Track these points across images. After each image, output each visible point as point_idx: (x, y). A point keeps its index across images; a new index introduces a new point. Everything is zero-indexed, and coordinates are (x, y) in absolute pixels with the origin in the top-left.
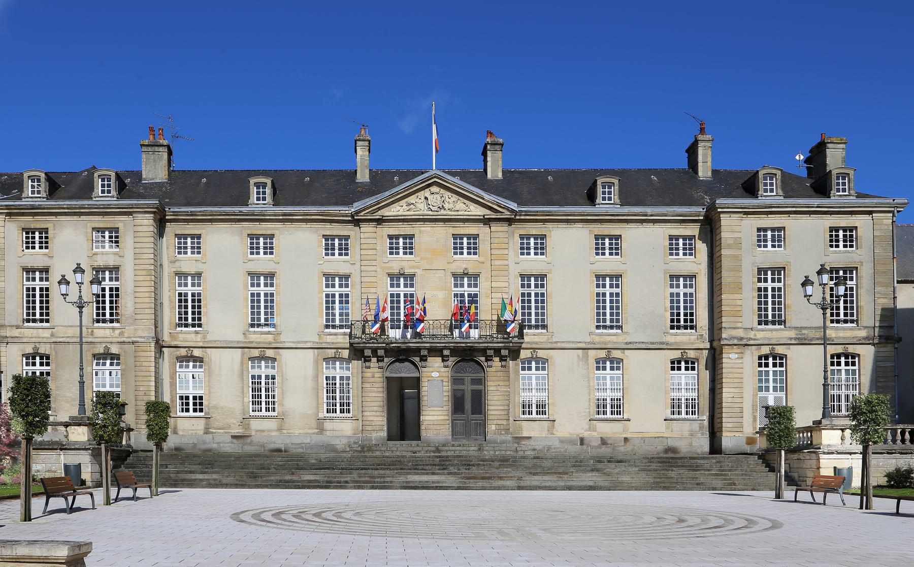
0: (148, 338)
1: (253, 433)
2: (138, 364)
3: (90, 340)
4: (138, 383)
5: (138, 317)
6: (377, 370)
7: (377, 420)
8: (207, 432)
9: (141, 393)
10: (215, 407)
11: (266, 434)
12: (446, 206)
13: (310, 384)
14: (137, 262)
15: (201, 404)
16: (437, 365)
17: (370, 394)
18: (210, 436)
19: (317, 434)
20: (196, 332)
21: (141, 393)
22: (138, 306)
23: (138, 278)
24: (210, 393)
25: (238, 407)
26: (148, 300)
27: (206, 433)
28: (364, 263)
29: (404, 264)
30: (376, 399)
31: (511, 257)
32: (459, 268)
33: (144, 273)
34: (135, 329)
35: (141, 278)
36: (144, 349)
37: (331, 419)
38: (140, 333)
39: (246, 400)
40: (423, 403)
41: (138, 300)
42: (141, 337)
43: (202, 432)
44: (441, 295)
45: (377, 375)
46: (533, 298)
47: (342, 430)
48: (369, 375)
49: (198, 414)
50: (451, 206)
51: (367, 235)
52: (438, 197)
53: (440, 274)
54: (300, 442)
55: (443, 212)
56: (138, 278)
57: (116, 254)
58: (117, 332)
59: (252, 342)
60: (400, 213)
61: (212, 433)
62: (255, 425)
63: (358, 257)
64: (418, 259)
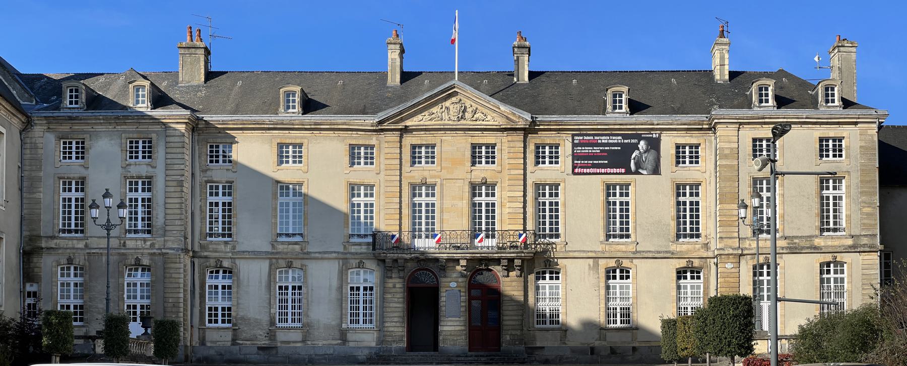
0: (178, 249)
1: (279, 344)
4: (167, 295)
5: (168, 228)
6: (398, 280)
7: (397, 328)
8: (234, 341)
9: (170, 305)
10: (243, 318)
11: (292, 345)
13: (334, 294)
15: (229, 315)
17: (391, 305)
18: (237, 347)
20: (226, 243)
21: (170, 305)
23: (169, 189)
24: (238, 304)
25: (265, 319)
27: (233, 345)
29: (426, 174)
33: (175, 184)
35: (172, 189)
37: (354, 329)
38: (169, 245)
39: (272, 311)
41: (169, 211)
43: (229, 344)
46: (547, 207)
47: (365, 338)
48: (391, 285)
49: (227, 325)
55: (462, 122)
56: (169, 189)
58: (148, 243)
60: (421, 123)
62: (281, 336)
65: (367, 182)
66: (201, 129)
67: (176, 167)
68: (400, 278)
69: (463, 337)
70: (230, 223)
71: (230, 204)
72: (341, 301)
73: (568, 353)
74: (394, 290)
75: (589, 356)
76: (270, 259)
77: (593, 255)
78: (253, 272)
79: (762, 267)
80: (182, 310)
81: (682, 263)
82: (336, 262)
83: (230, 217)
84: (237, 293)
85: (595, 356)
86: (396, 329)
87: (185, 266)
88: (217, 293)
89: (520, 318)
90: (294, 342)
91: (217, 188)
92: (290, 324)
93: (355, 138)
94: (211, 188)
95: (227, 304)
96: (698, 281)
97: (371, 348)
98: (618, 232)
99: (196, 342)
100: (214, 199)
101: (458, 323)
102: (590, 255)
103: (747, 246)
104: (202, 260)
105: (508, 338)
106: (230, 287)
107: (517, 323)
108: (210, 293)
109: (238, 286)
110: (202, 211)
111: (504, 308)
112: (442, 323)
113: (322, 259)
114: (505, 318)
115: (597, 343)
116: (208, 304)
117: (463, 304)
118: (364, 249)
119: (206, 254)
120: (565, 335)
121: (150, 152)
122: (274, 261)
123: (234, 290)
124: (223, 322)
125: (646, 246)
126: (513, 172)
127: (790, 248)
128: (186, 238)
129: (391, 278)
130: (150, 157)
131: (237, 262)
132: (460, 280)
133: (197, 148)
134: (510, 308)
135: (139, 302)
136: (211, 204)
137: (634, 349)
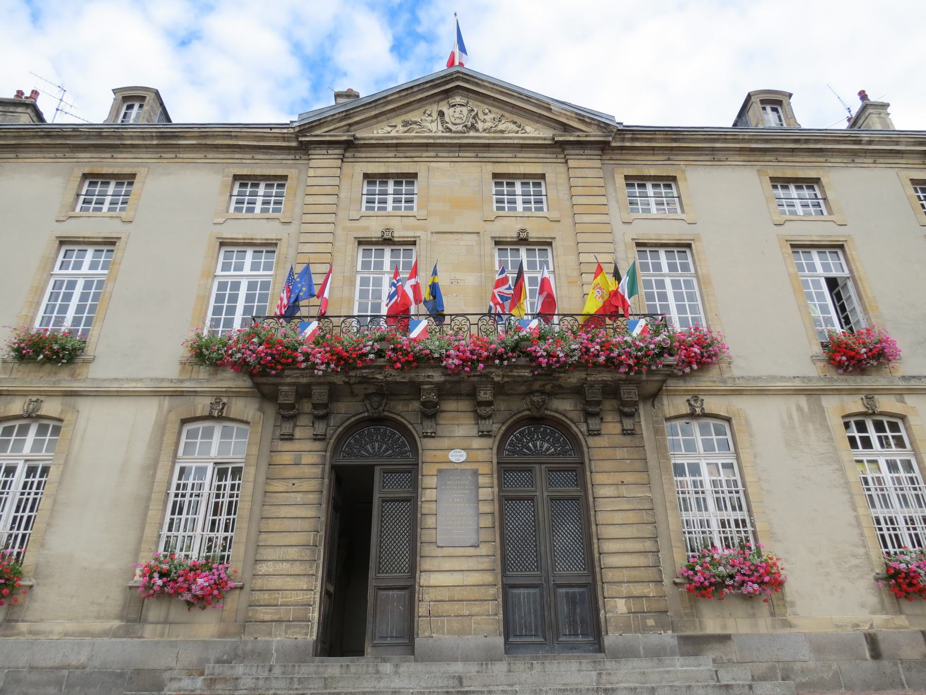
6: (309, 445)
12: (480, 125)
16: (461, 431)
19: (114, 634)
30: (298, 525)
40: (425, 536)
45: (307, 459)
50: (488, 125)
52: (465, 110)
55: (472, 134)
68: (316, 438)
69: (490, 607)
75: (870, 663)
82: (154, 403)
85: (886, 664)
97: (206, 644)
101: (472, 564)
105: (621, 606)
111: (601, 518)
112: (426, 564)
129: (290, 438)
132: (477, 443)
134: (618, 518)
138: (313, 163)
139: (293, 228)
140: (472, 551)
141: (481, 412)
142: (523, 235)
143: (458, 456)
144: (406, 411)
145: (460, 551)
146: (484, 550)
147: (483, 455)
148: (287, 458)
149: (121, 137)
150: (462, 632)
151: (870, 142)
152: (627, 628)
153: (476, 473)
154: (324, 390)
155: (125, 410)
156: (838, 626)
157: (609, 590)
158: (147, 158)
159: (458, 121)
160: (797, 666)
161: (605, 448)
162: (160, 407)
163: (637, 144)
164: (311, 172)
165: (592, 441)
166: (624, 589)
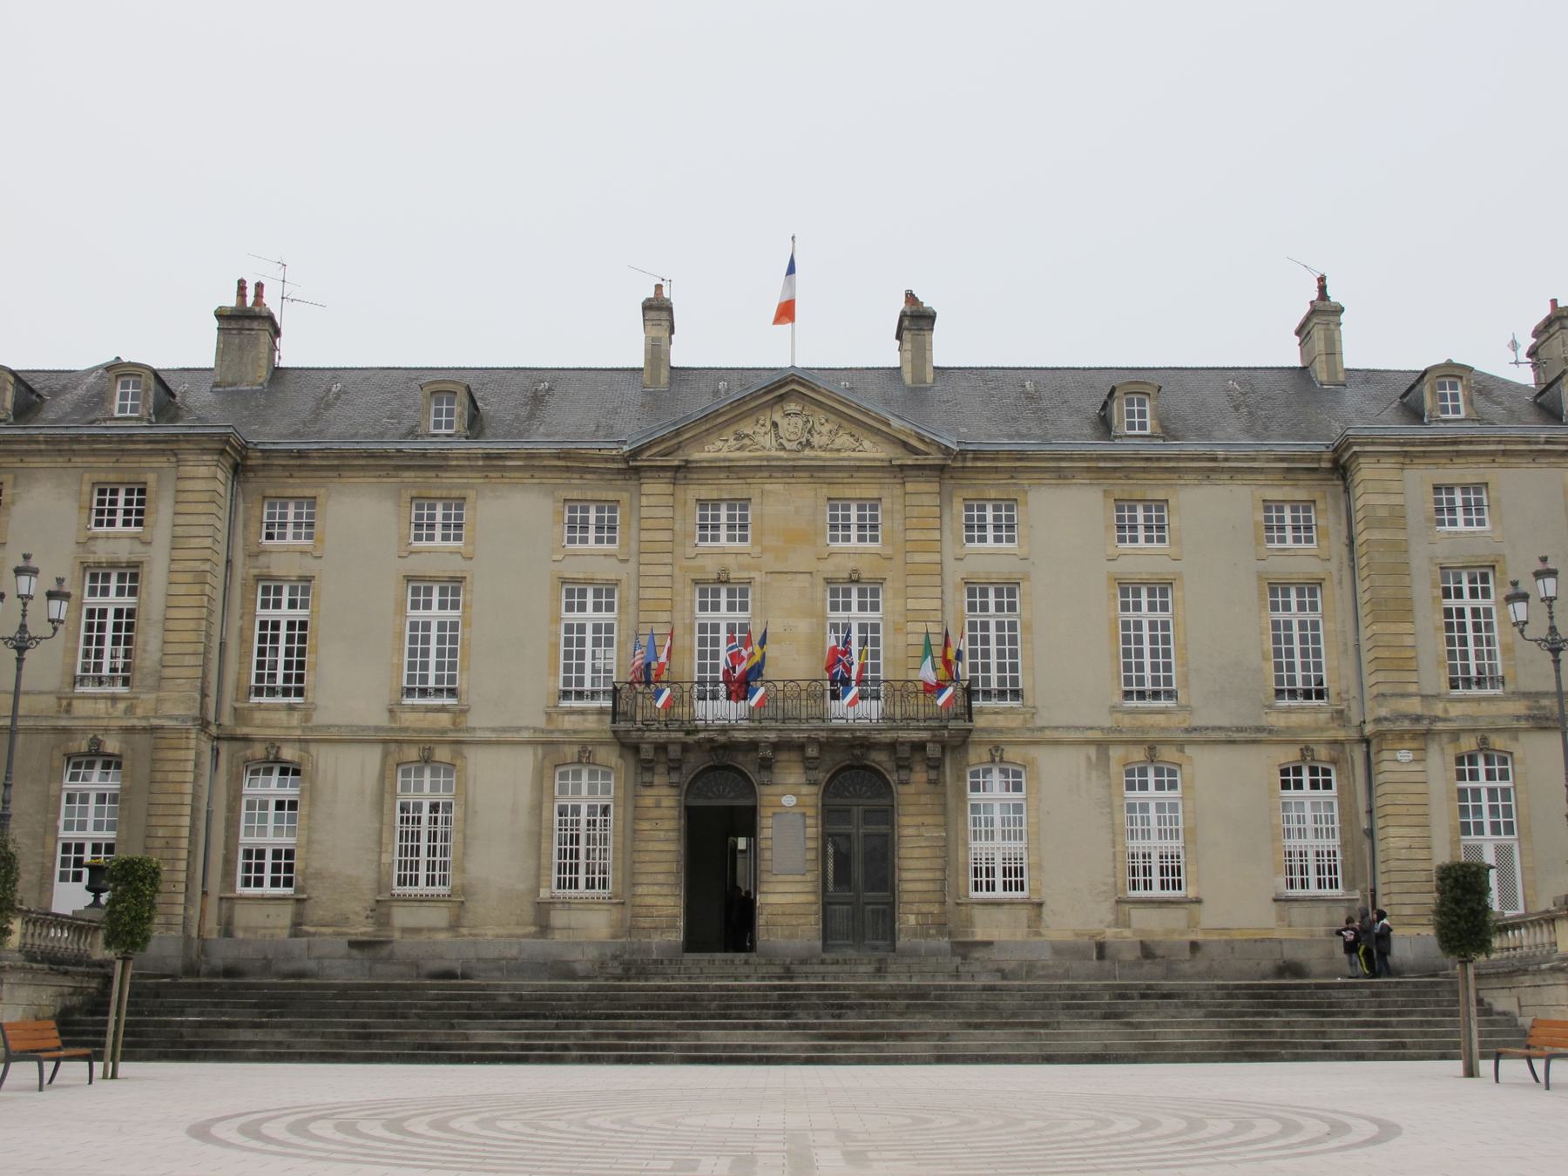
0: (184, 719)
1: (397, 935)
2: (159, 776)
3: (63, 723)
4: (154, 821)
5: (168, 672)
6: (666, 791)
7: (663, 900)
8: (297, 928)
9: (158, 843)
10: (319, 875)
12: (816, 440)
14: (178, 554)
15: (289, 868)
17: (651, 846)
19: (534, 936)
20: (291, 708)
21: (158, 843)
22: (170, 649)
23: (176, 589)
24: (309, 842)
26: (191, 636)
28: (645, 558)
29: (729, 561)
30: (663, 857)
31: (950, 549)
32: (839, 567)
33: (189, 577)
34: (159, 701)
35: (182, 589)
36: (175, 743)
37: (567, 903)
38: (168, 708)
39: (385, 859)
40: (763, 866)
41: (171, 637)
42: (170, 717)
43: (286, 932)
44: (803, 626)
45: (666, 802)
46: (993, 633)
47: (589, 925)
49: (281, 891)
50: (825, 440)
51: (653, 500)
53: (803, 581)
54: (496, 954)
55: (807, 452)
56: (176, 589)
57: (135, 537)
58: (121, 706)
59: (406, 729)
60: (721, 455)
61: (308, 934)
62: (402, 917)
63: (634, 545)
64: (758, 549)
65: (600, 576)
66: (252, 469)
67: (194, 542)
68: (672, 785)
69: (812, 919)
70: (301, 665)
71: (303, 625)
72: (537, 838)
73: (1047, 956)
74: (656, 813)
75: (1095, 963)
76: (385, 742)
77: (1097, 735)
78: (348, 775)
79: (1472, 760)
80: (184, 854)
81: (1290, 755)
83: (302, 652)
84: (310, 816)
85: (1107, 964)
86: (660, 901)
87: (198, 755)
88: (263, 818)
89: (938, 875)
90: (430, 930)
91: (278, 591)
92: (422, 888)
93: (577, 487)
94: (266, 590)
95: (285, 842)
96: (1327, 793)
97: (603, 944)
98: (1148, 686)
99: (212, 925)
100: (270, 614)
101: (799, 887)
102: (1090, 735)
103: (1440, 714)
104: (236, 745)
105: (912, 920)
106: (293, 805)
107: (931, 886)
108: (250, 818)
109: (312, 803)
110: (244, 640)
111: (903, 852)
112: (764, 888)
113: (498, 743)
114: (905, 875)
115: (1110, 934)
116: (246, 840)
117: (811, 844)
118: (591, 722)
119: (245, 730)
120: (1039, 916)
121: (140, 512)
122: (393, 747)
123: (302, 810)
124: (275, 882)
125: (1210, 716)
126: (918, 558)
127: (1534, 717)
128: (204, 695)
129: (650, 785)
130: (139, 523)
131: (313, 748)
132: (805, 790)
133: (241, 507)
134: (916, 853)
135: (90, 835)
136: (263, 625)
137: (1195, 946)
138: (646, 488)
139: (632, 565)
140: (798, 878)
141: (809, 765)
142: (854, 577)
143: (789, 801)
144: (746, 763)
145: (790, 878)
146: (809, 877)
147: (810, 800)
148: (649, 802)
149: (446, 458)
150: (792, 936)
151: (1226, 460)
152: (915, 935)
153: (804, 815)
154: (678, 748)
155: (504, 754)
156: (1077, 935)
157: (902, 908)
158: (476, 479)
159: (793, 437)
160: (1039, 964)
161: (912, 792)
162: (535, 755)
163: (979, 464)
164: (644, 501)
165: (902, 789)
166: (915, 908)
